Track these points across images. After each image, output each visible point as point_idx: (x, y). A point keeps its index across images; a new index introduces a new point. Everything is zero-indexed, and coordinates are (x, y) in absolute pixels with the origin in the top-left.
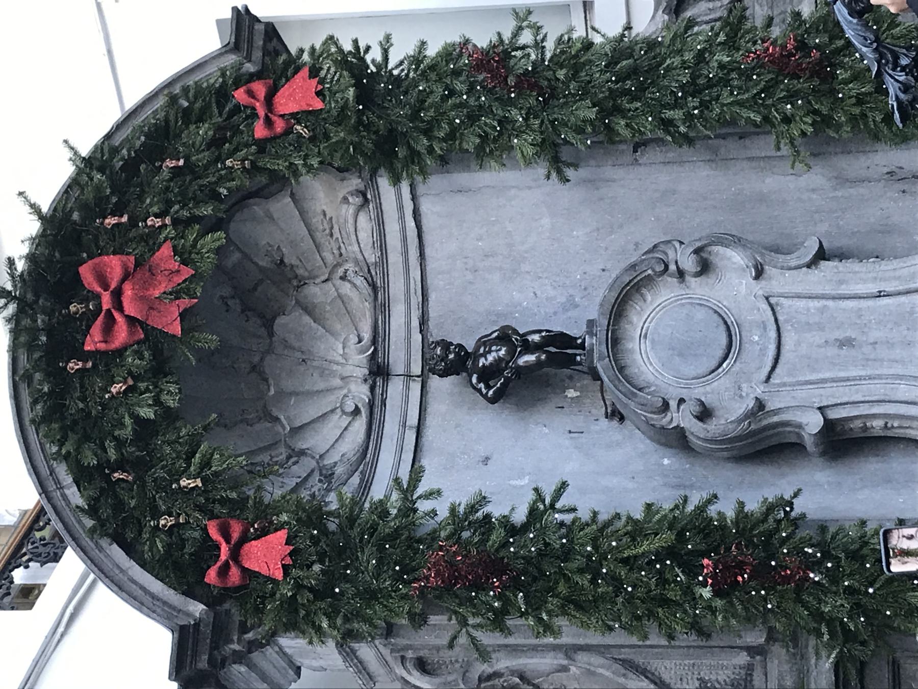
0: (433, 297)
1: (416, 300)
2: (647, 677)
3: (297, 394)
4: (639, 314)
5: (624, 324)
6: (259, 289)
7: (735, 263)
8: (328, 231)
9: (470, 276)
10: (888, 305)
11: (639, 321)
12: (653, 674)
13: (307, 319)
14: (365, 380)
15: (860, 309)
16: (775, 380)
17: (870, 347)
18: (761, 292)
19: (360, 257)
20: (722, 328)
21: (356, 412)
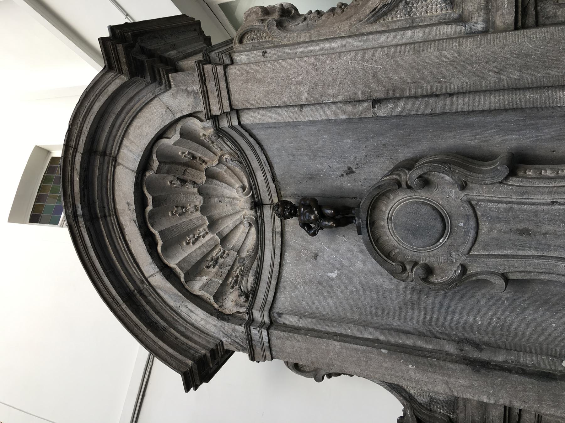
0: (275, 166)
1: (267, 168)
2: (402, 396)
3: (221, 218)
4: (386, 206)
5: (377, 212)
6: (187, 173)
7: (446, 180)
8: (210, 142)
9: (291, 158)
10: (559, 209)
11: (386, 210)
12: (405, 391)
13: (215, 182)
14: (251, 209)
15: (537, 211)
16: (473, 253)
17: (542, 236)
18: (465, 198)
19: (231, 151)
20: (439, 219)
21: (250, 225)
